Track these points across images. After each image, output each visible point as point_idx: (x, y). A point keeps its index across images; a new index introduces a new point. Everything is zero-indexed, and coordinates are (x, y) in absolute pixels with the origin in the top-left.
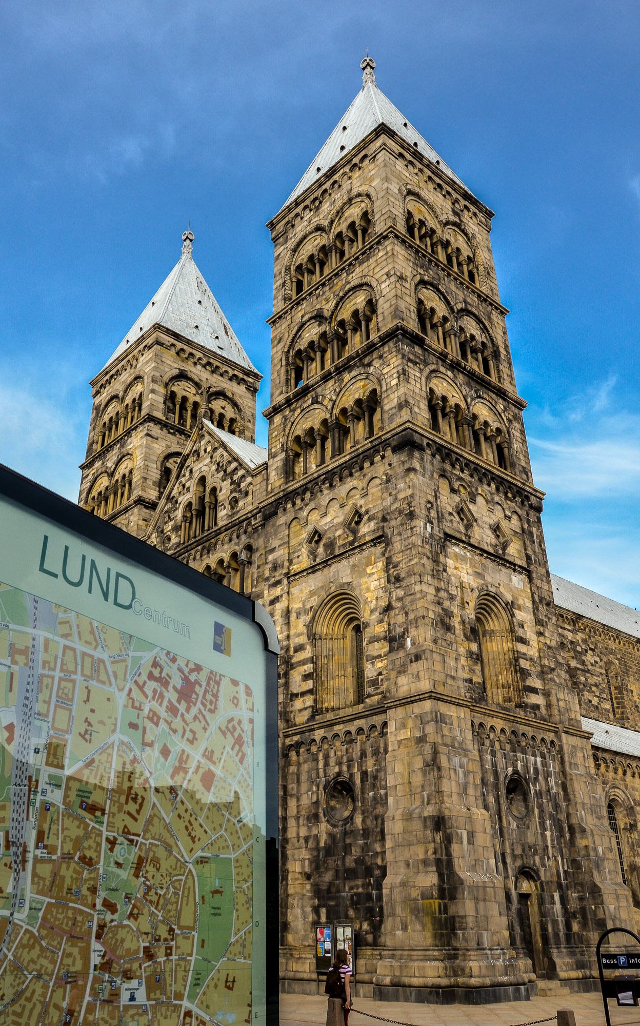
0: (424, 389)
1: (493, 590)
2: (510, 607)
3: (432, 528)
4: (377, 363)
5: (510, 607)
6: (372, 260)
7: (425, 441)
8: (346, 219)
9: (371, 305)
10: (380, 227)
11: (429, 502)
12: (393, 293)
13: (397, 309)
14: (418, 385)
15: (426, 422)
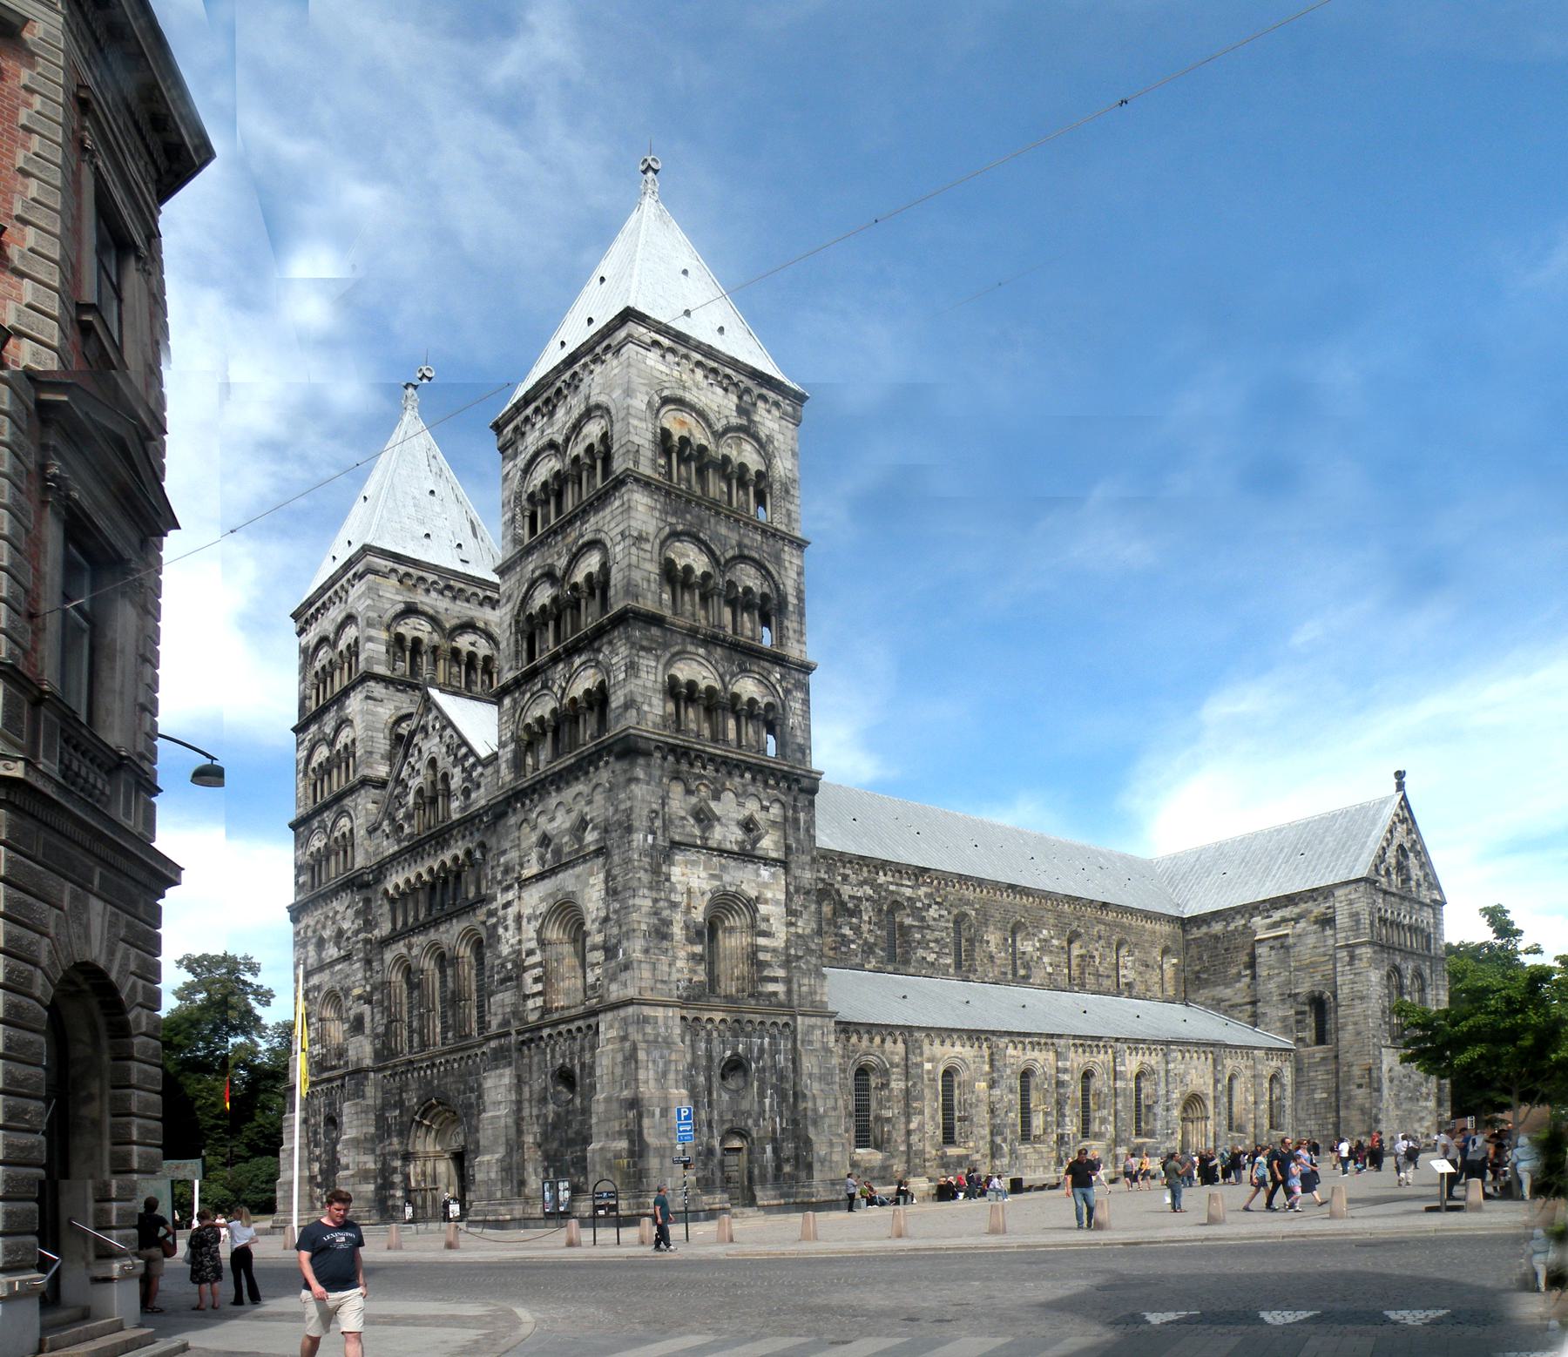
0: (660, 679)
1: (733, 889)
2: (752, 904)
3: (654, 839)
4: (606, 650)
5: (752, 904)
6: (608, 510)
7: (653, 745)
8: (584, 439)
9: (605, 568)
10: (618, 466)
11: (653, 811)
12: (626, 562)
13: (629, 584)
14: (652, 677)
15: (658, 720)
